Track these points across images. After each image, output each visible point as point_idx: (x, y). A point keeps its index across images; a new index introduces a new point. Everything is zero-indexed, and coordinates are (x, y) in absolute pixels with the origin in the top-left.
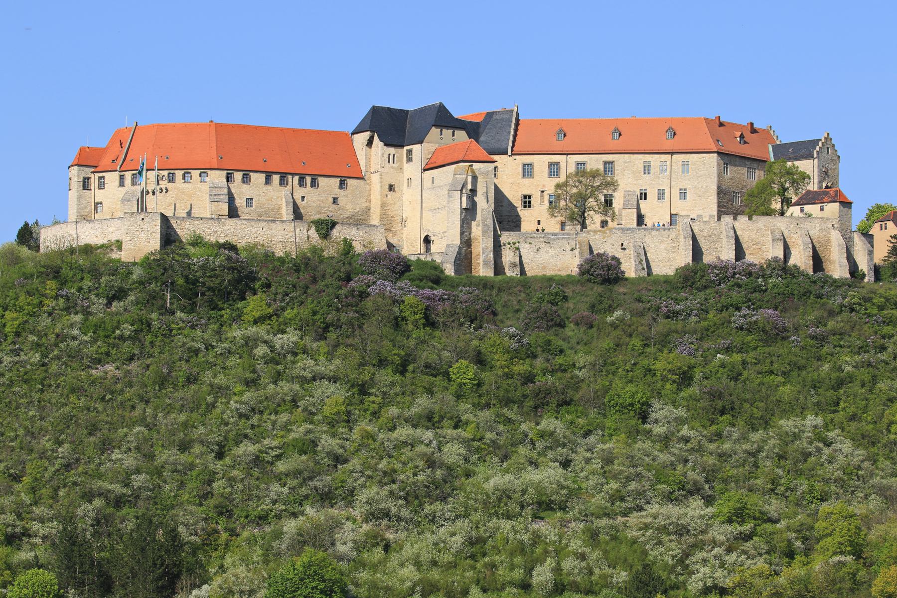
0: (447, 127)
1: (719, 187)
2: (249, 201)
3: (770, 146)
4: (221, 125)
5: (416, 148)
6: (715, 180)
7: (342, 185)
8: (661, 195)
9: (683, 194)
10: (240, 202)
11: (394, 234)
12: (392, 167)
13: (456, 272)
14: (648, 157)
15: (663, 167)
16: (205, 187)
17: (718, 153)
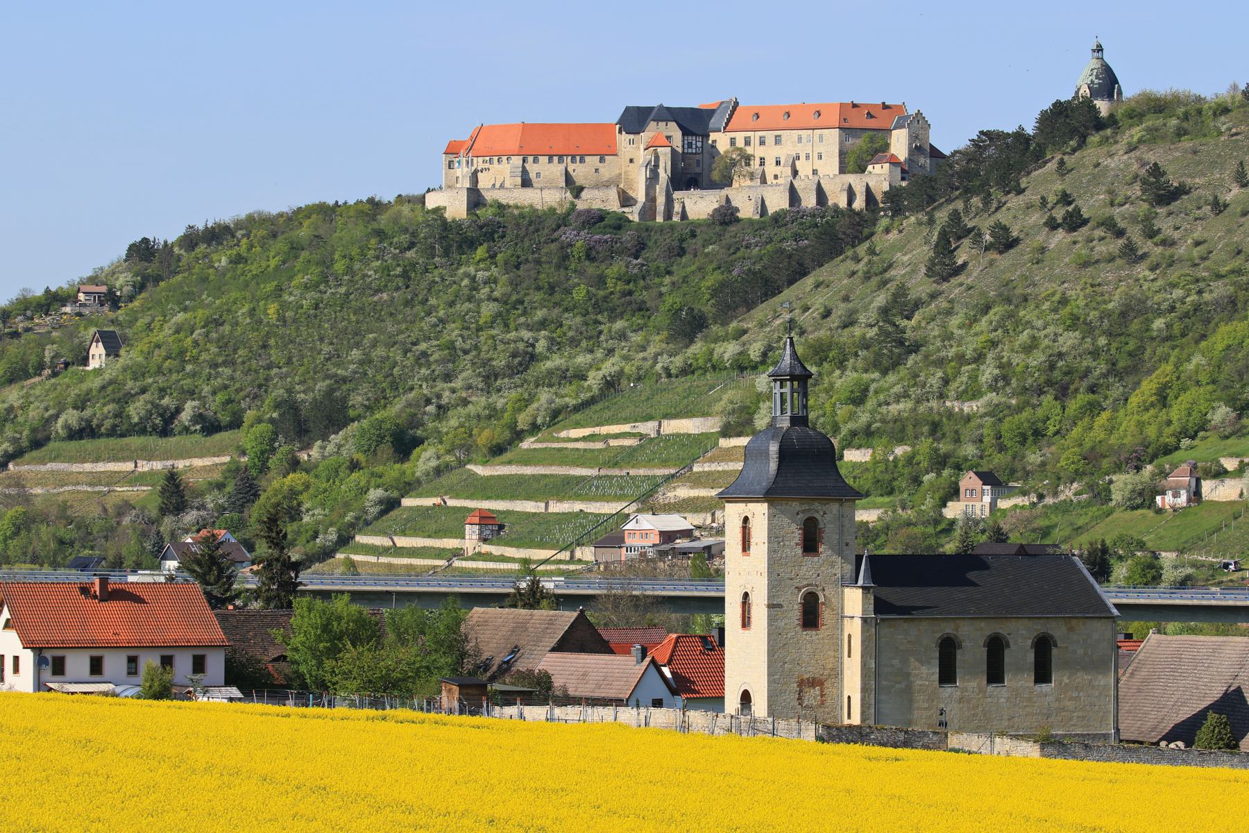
0: (662, 121)
1: (840, 151)
2: (538, 175)
7: (602, 160)
8: (807, 157)
9: (820, 157)
10: (532, 176)
11: (634, 191)
13: (640, 219)
14: (800, 132)
16: (508, 166)
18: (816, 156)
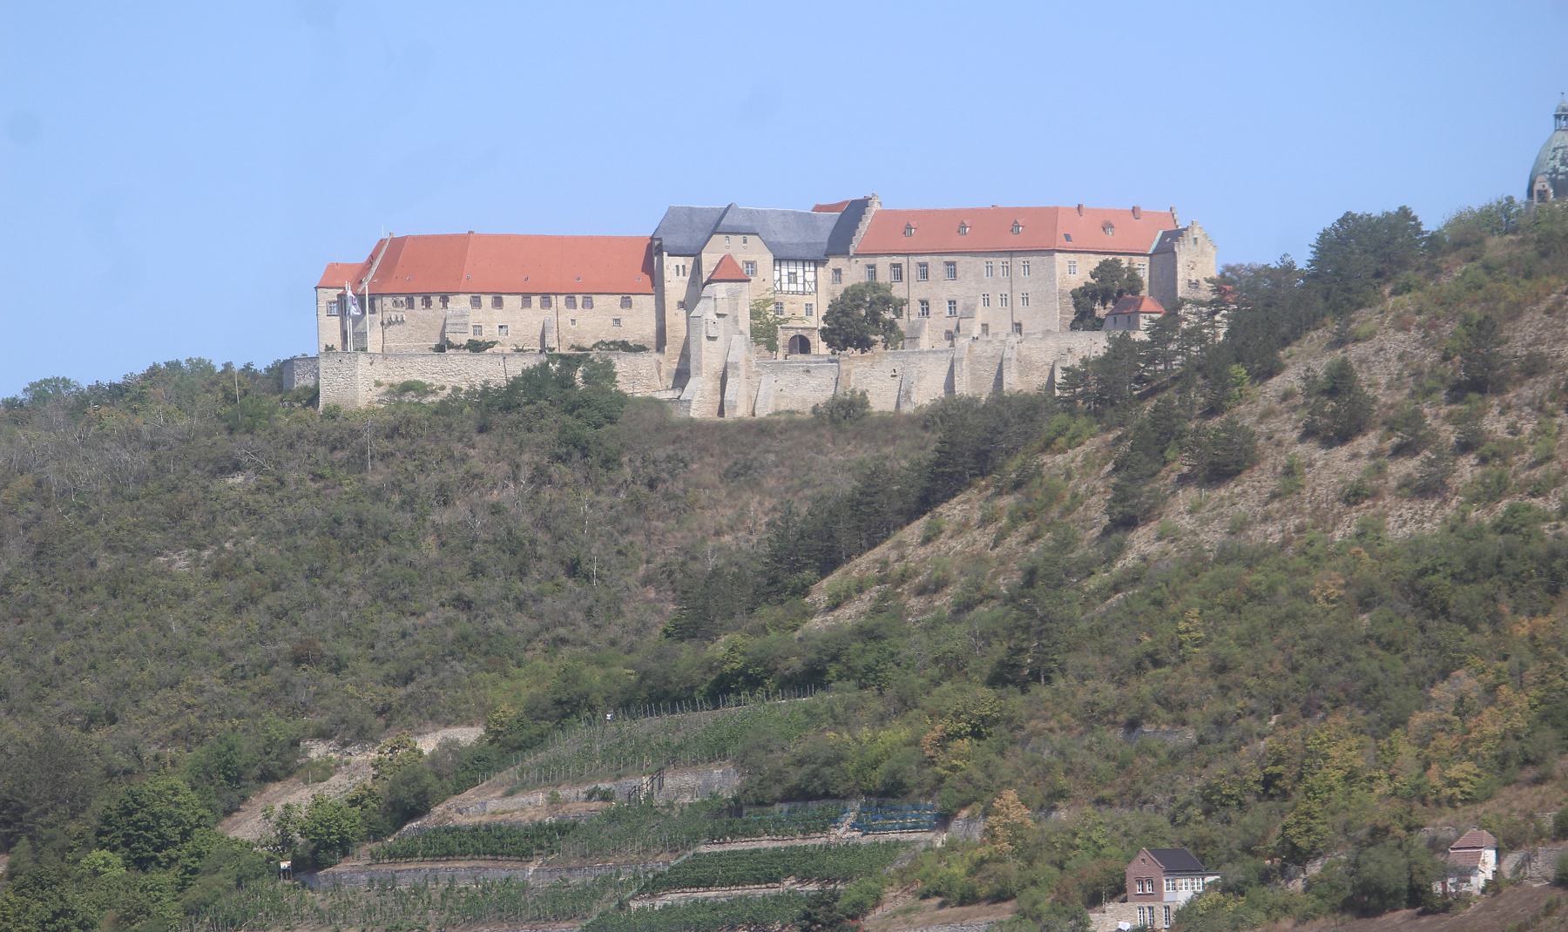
7: (627, 303)
12: (682, 281)
18: (1018, 298)
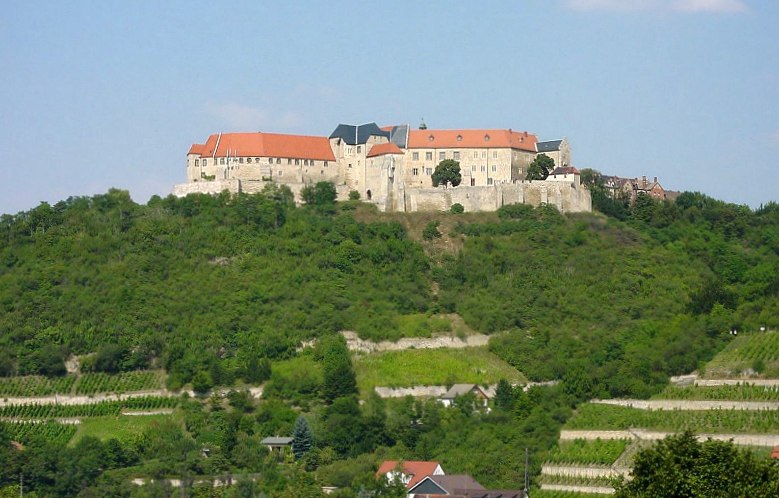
0: (378, 135)
1: (512, 165)
3: (535, 144)
4: (265, 134)
5: (362, 146)
6: (510, 162)
7: (326, 164)
9: (494, 169)
14: (476, 150)
15: (484, 155)
17: (512, 148)
